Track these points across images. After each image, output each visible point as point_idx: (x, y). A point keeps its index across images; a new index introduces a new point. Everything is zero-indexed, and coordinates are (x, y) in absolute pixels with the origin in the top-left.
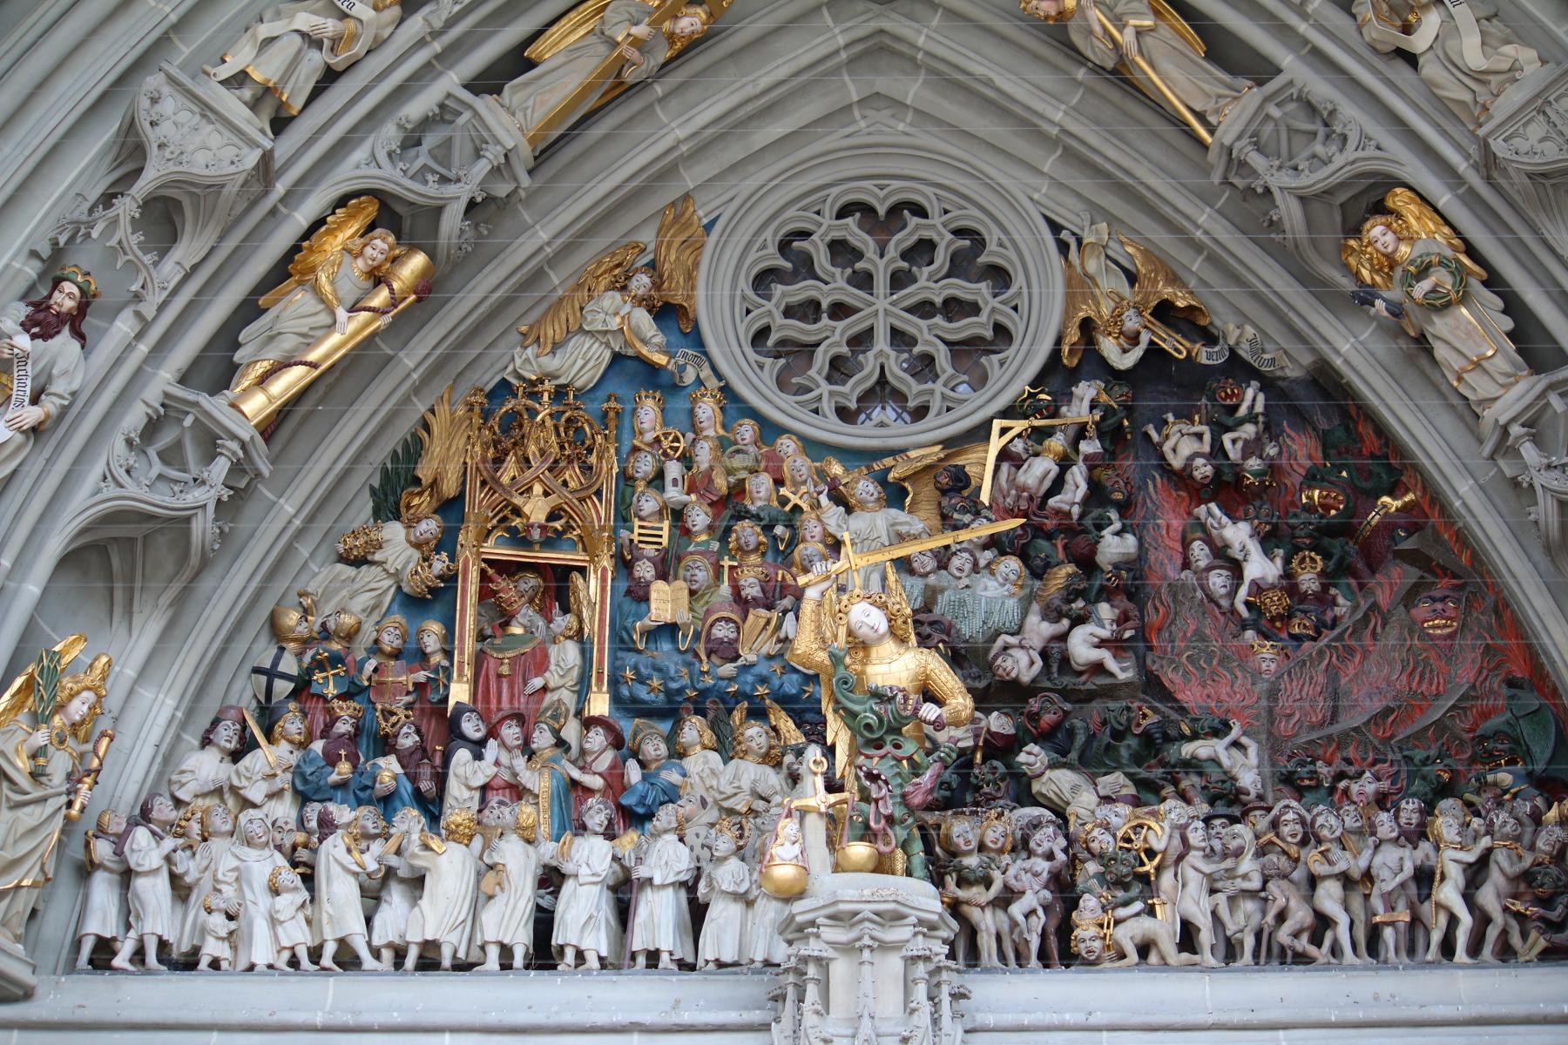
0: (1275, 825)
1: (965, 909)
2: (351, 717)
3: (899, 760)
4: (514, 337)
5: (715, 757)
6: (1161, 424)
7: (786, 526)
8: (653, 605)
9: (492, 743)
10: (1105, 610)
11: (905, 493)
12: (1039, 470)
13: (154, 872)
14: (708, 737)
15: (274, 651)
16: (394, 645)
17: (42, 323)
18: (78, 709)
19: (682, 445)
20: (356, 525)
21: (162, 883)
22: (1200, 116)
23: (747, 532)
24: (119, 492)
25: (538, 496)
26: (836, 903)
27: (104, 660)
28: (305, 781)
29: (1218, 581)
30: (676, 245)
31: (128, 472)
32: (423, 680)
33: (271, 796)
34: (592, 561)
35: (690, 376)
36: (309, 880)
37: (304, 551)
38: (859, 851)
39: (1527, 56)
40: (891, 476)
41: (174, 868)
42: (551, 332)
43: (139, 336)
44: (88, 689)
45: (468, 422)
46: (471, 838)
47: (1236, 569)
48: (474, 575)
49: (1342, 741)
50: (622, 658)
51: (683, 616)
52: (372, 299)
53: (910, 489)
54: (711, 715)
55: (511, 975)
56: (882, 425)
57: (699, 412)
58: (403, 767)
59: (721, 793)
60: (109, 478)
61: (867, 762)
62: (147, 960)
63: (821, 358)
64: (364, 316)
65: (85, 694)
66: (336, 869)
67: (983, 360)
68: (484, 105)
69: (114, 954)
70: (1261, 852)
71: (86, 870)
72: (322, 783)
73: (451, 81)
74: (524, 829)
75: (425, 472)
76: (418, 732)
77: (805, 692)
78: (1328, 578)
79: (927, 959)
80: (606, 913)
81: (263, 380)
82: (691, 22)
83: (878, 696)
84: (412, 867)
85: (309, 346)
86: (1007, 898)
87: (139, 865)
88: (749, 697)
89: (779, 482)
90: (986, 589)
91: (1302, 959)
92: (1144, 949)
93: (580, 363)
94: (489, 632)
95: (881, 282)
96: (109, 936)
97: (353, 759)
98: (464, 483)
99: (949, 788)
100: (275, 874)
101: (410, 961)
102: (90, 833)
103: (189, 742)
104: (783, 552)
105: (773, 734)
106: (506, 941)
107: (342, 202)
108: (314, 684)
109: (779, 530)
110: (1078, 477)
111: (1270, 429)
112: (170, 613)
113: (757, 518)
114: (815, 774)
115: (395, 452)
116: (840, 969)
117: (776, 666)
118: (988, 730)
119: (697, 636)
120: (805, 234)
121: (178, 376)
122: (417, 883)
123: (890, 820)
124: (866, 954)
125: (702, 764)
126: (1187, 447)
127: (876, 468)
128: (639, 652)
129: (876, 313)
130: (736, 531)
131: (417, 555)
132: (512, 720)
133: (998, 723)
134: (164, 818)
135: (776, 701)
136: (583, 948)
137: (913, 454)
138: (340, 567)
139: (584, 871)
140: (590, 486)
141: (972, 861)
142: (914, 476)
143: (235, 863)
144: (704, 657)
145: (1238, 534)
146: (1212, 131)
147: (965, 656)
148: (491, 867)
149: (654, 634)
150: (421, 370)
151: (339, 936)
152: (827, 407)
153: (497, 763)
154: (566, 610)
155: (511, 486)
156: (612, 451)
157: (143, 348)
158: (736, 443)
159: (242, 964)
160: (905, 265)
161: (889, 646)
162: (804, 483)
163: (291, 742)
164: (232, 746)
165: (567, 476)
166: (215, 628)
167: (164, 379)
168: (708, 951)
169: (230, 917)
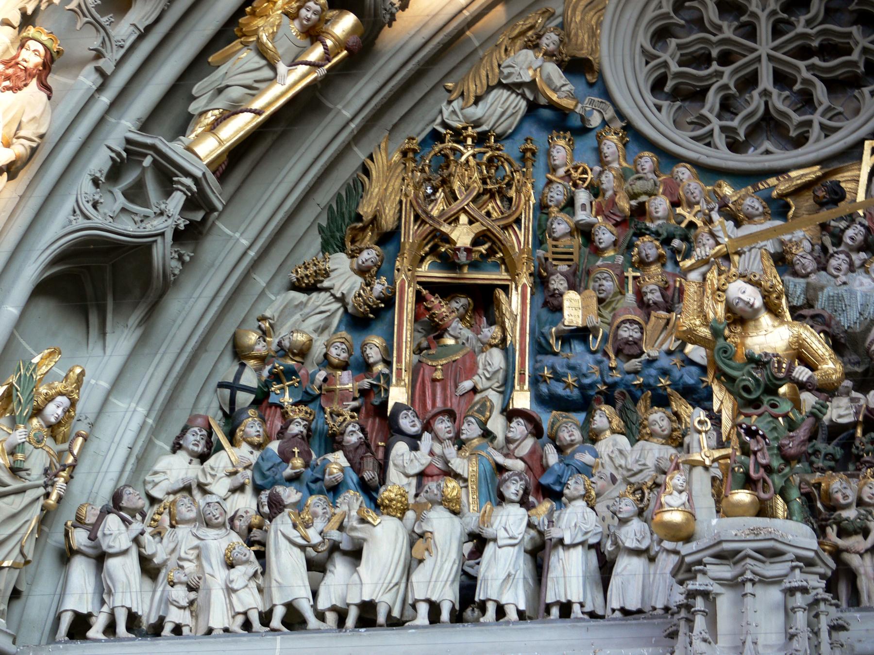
1: (846, 556)
2: (303, 419)
3: (776, 417)
4: (441, 93)
5: (623, 441)
7: (682, 240)
8: (566, 312)
9: (427, 436)
11: (789, 207)
13: (124, 553)
14: (616, 422)
15: (236, 368)
16: (341, 358)
18: (53, 411)
19: (590, 176)
20: (307, 259)
21: (132, 563)
23: (648, 247)
24: (87, 223)
25: (464, 224)
26: (720, 542)
27: (78, 370)
28: (264, 476)
30: (580, 7)
31: (95, 206)
32: (367, 386)
33: (233, 491)
34: (513, 279)
35: (595, 121)
36: (261, 556)
37: (261, 280)
41: (143, 550)
43: (101, 89)
44: (61, 394)
45: (403, 166)
46: (403, 512)
48: (410, 295)
50: (541, 361)
51: (594, 320)
52: (308, 55)
53: (791, 203)
54: (619, 404)
55: (436, 630)
56: (767, 152)
57: (605, 150)
58: (349, 460)
59: (629, 470)
60: (78, 212)
61: (747, 421)
62: (118, 630)
63: (713, 99)
64: (303, 69)
65: (59, 399)
66: (283, 543)
67: (856, 93)
69: (89, 627)
71: (66, 555)
72: (277, 477)
74: (450, 501)
76: (362, 430)
77: (703, 382)
79: (804, 590)
80: (522, 567)
83: (757, 362)
84: (352, 539)
87: (110, 547)
88: (653, 389)
89: (675, 204)
90: (861, 284)
93: (500, 110)
94: (425, 344)
95: (764, 29)
96: (85, 612)
97: (305, 455)
98: (400, 218)
99: (833, 458)
100: (230, 549)
101: (351, 621)
102: (69, 523)
103: (162, 448)
105: (674, 418)
106: (434, 599)
108: (272, 394)
109: (676, 243)
112: (138, 333)
113: (657, 234)
114: (700, 432)
115: (339, 195)
116: (725, 602)
117: (676, 359)
118: (867, 408)
119: (605, 339)
121: (139, 124)
123: (768, 469)
124: (749, 588)
127: (761, 187)
128: (556, 354)
129: (758, 59)
130: (637, 246)
131: (359, 281)
132: (443, 416)
134: (133, 506)
135: (677, 390)
136: (503, 602)
137: (793, 174)
138: (293, 294)
139: (502, 534)
140: (510, 216)
141: (851, 514)
142: (799, 191)
143: (196, 542)
144: (612, 356)
147: (844, 345)
148: (421, 536)
150: (358, 120)
151: (286, 601)
152: (719, 139)
153: (431, 453)
154: (491, 323)
155: (440, 216)
156: (529, 185)
157: (105, 99)
158: (637, 172)
159: (203, 630)
160: (785, 16)
161: (765, 319)
162: (698, 203)
163: (251, 444)
164: (200, 449)
165: (490, 207)
166: (180, 346)
169: (191, 589)
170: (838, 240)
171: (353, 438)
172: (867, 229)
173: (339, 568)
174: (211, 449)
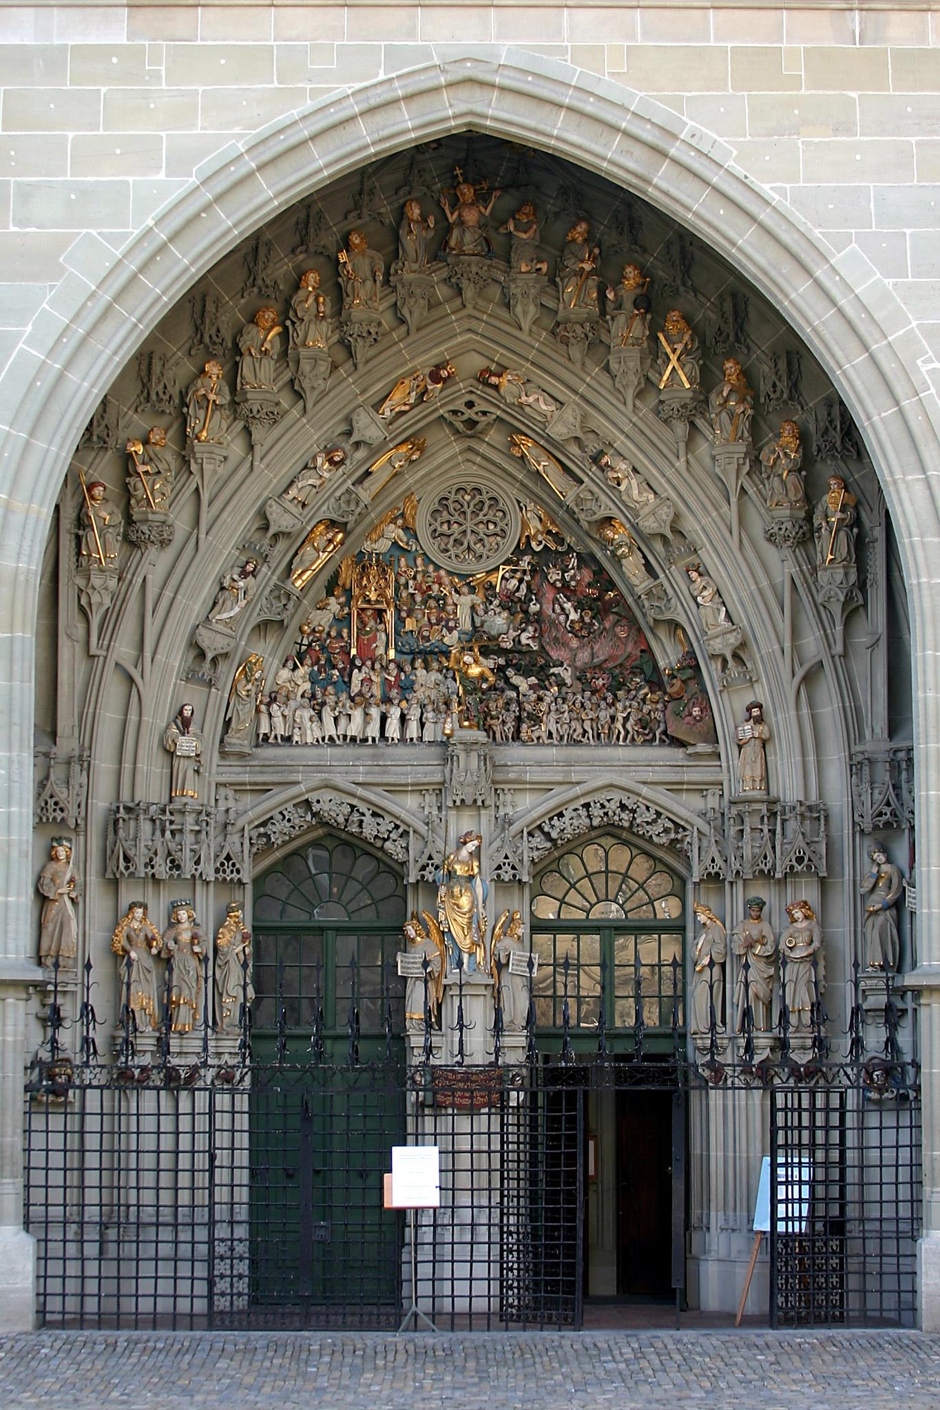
0: (574, 704)
6: (548, 568)
10: (531, 628)
12: (514, 582)
17: (244, 574)
18: (257, 675)
23: (432, 603)
29: (562, 618)
38: (466, 723)
39: (652, 496)
42: (374, 537)
47: (567, 616)
49: (595, 668)
51: (415, 629)
68: (359, 490)
70: (571, 711)
73: (350, 482)
75: (340, 583)
78: (593, 618)
81: (300, 576)
82: (414, 457)
86: (504, 722)
89: (440, 584)
91: (578, 743)
92: (538, 738)
104: (443, 609)
110: (524, 586)
111: (579, 568)
116: (462, 756)
120: (447, 499)
122: (349, 716)
125: (421, 672)
126: (555, 577)
133: (501, 661)
145: (568, 606)
167: (275, 578)
168: (426, 739)
170: (491, 603)
171: (341, 666)
173: (343, 721)
174: (295, 668)
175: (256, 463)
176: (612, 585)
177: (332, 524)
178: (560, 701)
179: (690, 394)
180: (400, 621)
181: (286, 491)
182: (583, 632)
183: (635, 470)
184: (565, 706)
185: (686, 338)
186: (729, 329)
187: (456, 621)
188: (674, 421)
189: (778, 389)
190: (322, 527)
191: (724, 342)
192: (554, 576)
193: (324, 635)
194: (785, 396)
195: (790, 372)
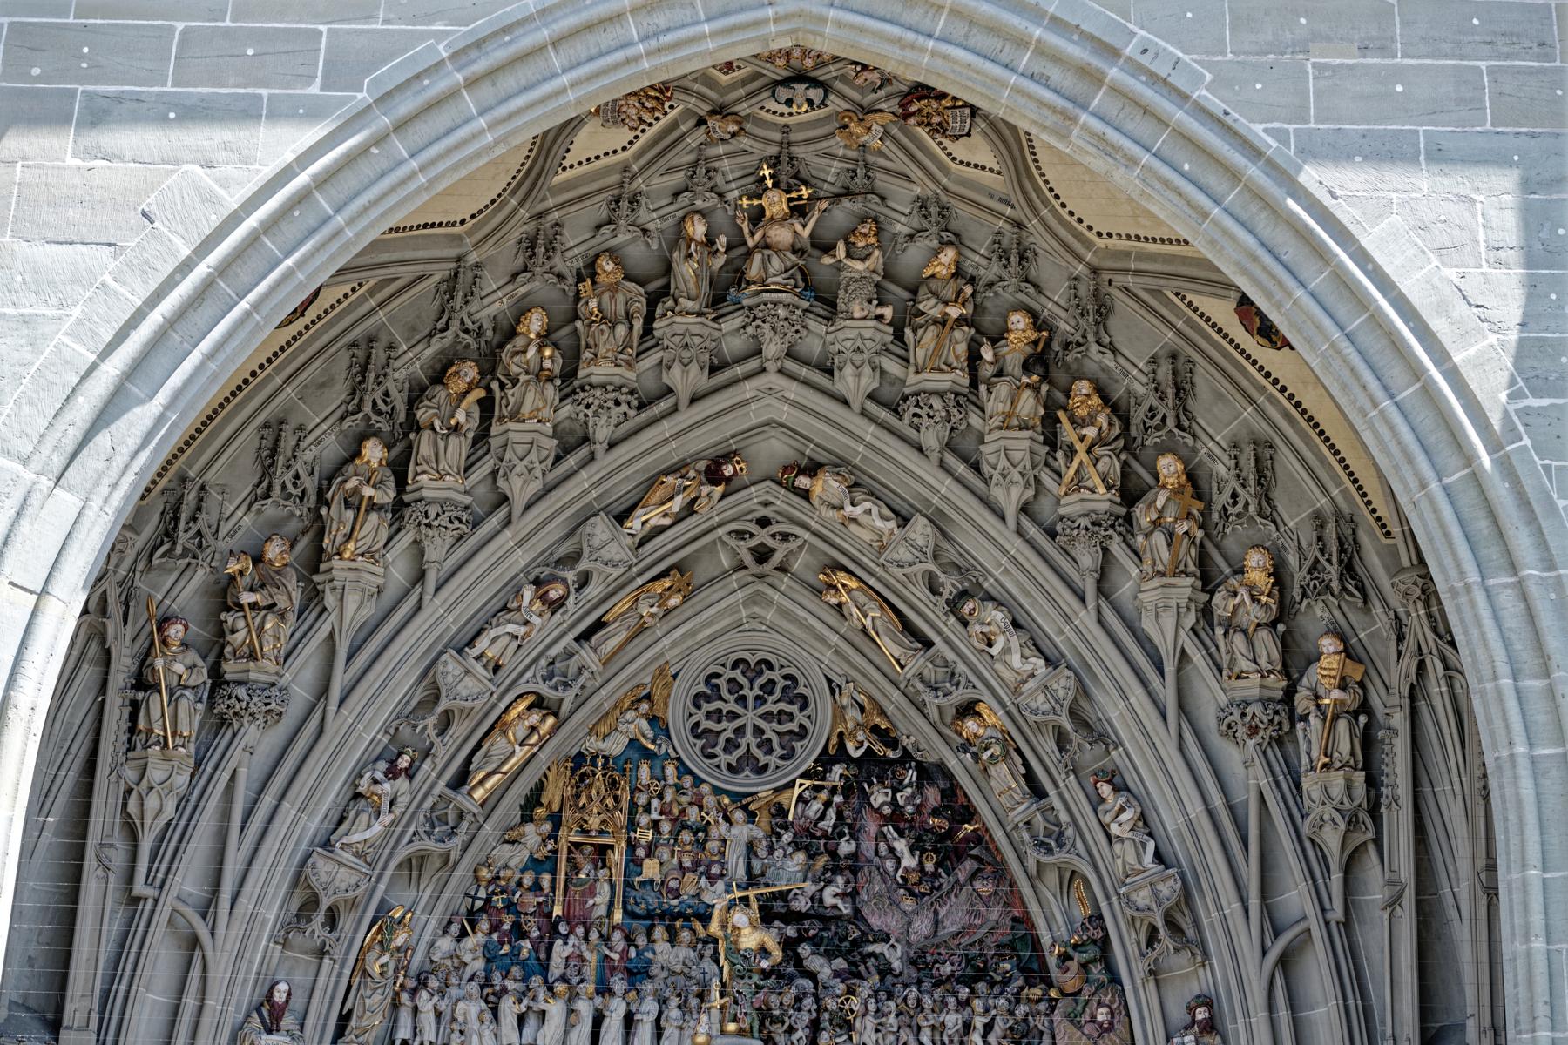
6: (871, 784)
10: (840, 880)
12: (816, 807)
22: (898, 661)
23: (686, 836)
29: (890, 865)
39: (1042, 662)
40: (752, 807)
47: (898, 861)
51: (658, 878)
78: (938, 864)
81: (481, 782)
85: (503, 763)
89: (701, 808)
104: (702, 845)
107: (520, 696)
109: (701, 834)
110: (831, 813)
111: (919, 786)
138: (507, 846)
145: (901, 845)
146: (902, 667)
149: (642, 883)
167: (442, 783)
170: (779, 837)
172: (795, 835)
175: (427, 598)
176: (969, 813)
177: (539, 703)
178: (882, 995)
179: (1106, 506)
180: (634, 863)
181: (471, 643)
182: (922, 887)
183: (1016, 624)
184: (892, 1004)
185: (1102, 419)
186: (1166, 409)
187: (722, 865)
188: (1079, 547)
189: (1240, 505)
190: (522, 706)
191: (1158, 428)
192: (879, 797)
193: (513, 884)
194: (1252, 509)
195: (1260, 475)
